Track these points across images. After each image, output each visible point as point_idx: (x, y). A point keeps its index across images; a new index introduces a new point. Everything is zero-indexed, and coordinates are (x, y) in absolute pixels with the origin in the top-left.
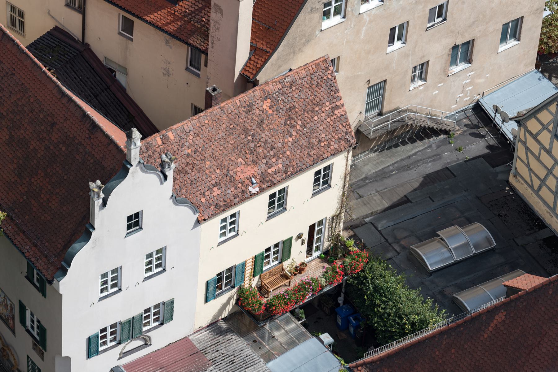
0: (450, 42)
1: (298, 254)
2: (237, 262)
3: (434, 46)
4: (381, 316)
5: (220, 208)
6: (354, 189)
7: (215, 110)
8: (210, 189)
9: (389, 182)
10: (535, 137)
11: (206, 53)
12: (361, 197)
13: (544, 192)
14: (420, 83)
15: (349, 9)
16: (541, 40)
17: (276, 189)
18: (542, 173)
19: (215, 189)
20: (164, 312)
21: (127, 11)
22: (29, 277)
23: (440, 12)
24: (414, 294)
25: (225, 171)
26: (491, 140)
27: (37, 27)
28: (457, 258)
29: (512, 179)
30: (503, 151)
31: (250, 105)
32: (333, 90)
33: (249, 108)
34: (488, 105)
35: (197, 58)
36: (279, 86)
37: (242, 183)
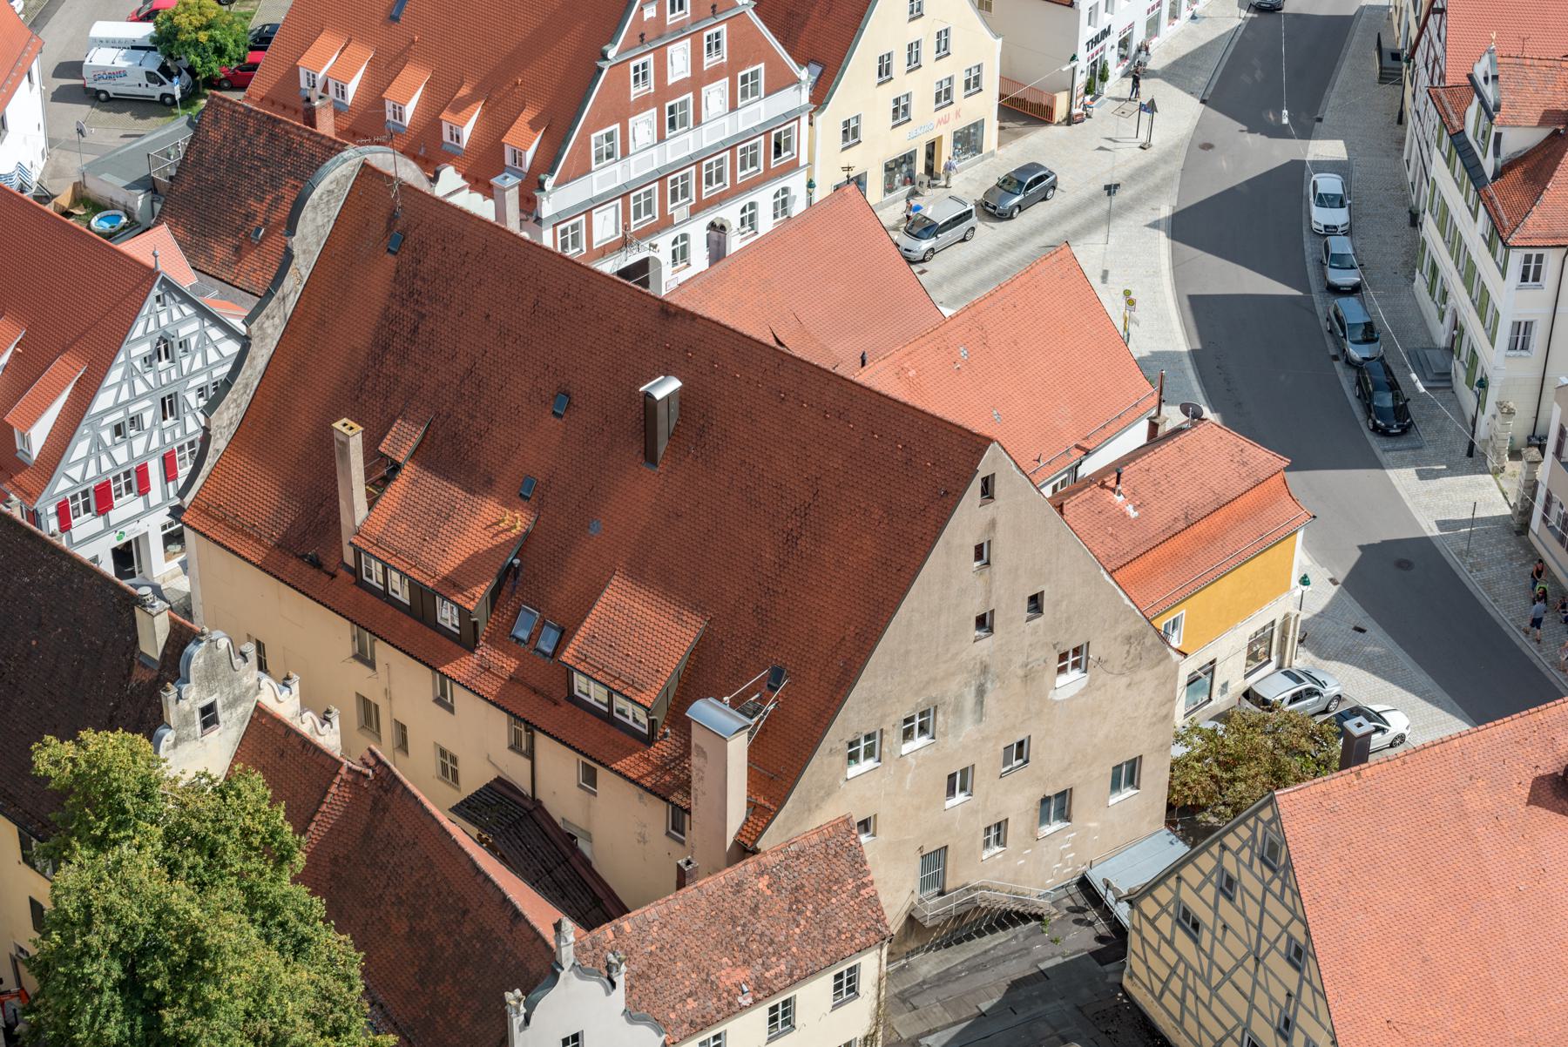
0: (1037, 793)
3: (1015, 798)
5: (697, 1027)
6: (897, 1000)
7: (690, 891)
8: (683, 1001)
9: (955, 988)
10: (1152, 922)
11: (688, 811)
12: (915, 1008)
13: (1168, 999)
14: (998, 849)
15: (885, 749)
16: (1171, 787)
18: (1164, 973)
19: (690, 1000)
21: (590, 758)
23: (1020, 749)
25: (704, 975)
26: (1102, 928)
27: (474, 778)
29: (1126, 982)
30: (1116, 942)
31: (740, 884)
32: (858, 861)
33: (739, 887)
34: (1096, 878)
35: (679, 820)
36: (781, 857)
37: (729, 992)
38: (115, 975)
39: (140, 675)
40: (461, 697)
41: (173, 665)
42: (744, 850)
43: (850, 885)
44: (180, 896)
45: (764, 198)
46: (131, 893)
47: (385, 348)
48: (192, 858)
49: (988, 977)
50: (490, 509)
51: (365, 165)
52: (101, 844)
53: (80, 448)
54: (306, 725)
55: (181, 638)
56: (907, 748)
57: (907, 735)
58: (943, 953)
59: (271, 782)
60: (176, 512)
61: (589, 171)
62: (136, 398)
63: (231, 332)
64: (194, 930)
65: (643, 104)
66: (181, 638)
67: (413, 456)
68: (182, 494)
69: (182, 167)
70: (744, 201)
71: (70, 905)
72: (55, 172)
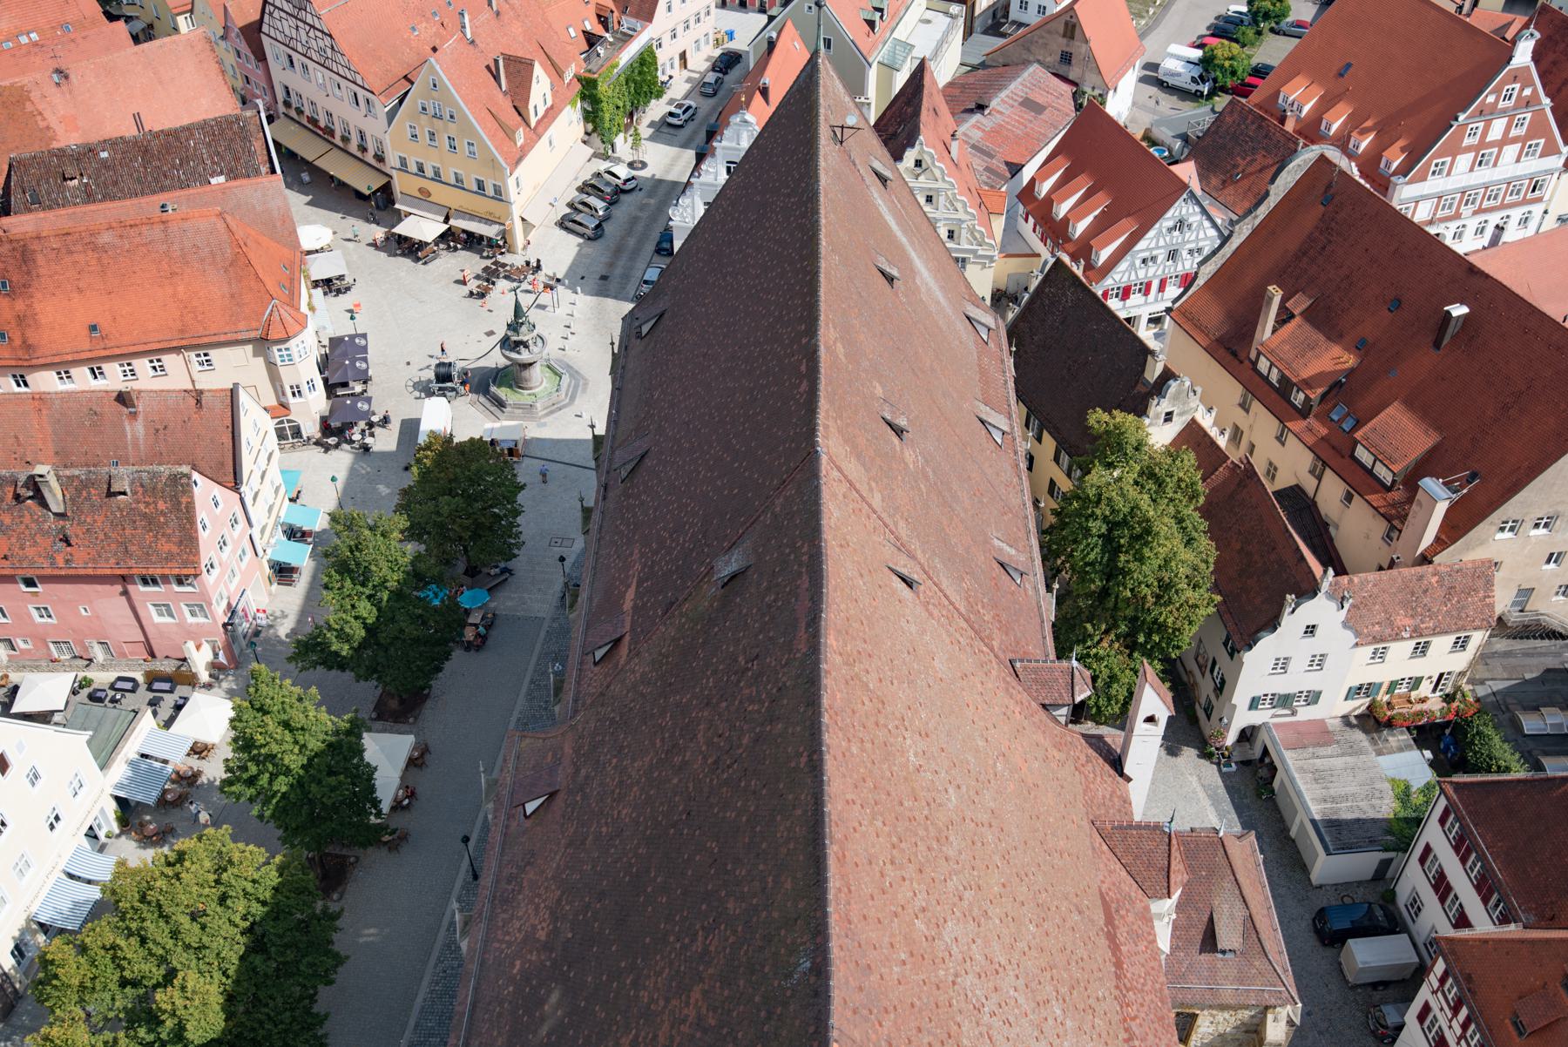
1: (1425, 689)
2: (1377, 681)
4: (1475, 753)
5: (1376, 640)
6: (1483, 657)
7: (1394, 572)
9: (1512, 661)
17: (1422, 640)
20: (1313, 698)
22: (1225, 644)
24: (1506, 746)
27: (1283, 481)
28: (1549, 731)
32: (1489, 583)
33: (1420, 578)
38: (1103, 530)
39: (1140, 388)
40: (1291, 440)
41: (1159, 387)
42: (1425, 559)
43: (1481, 594)
44: (1144, 501)
45: (1517, 214)
46: (1123, 495)
47: (1305, 254)
48: (1151, 485)
49: (1534, 661)
50: (1336, 350)
51: (1322, 156)
52: (1110, 466)
53: (1123, 265)
54: (1213, 432)
55: (1168, 375)
56: (1534, 532)
57: (1537, 526)
58: (1511, 641)
59: (1198, 458)
60: (1168, 310)
61: (1424, 179)
62: (1158, 247)
63: (1215, 225)
64: (1148, 520)
65: (1468, 149)
66: (1168, 375)
67: (1302, 314)
68: (1174, 302)
69: (1207, 133)
70: (1504, 213)
71: (1092, 492)
72: (1133, 120)
